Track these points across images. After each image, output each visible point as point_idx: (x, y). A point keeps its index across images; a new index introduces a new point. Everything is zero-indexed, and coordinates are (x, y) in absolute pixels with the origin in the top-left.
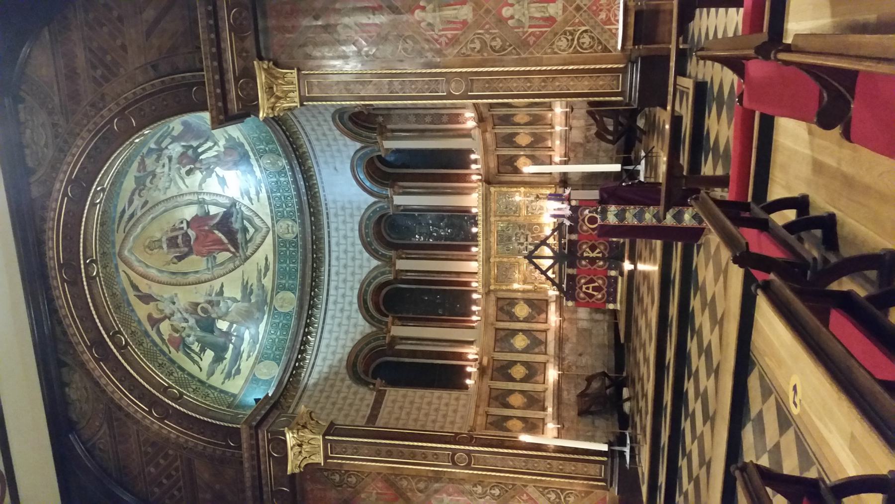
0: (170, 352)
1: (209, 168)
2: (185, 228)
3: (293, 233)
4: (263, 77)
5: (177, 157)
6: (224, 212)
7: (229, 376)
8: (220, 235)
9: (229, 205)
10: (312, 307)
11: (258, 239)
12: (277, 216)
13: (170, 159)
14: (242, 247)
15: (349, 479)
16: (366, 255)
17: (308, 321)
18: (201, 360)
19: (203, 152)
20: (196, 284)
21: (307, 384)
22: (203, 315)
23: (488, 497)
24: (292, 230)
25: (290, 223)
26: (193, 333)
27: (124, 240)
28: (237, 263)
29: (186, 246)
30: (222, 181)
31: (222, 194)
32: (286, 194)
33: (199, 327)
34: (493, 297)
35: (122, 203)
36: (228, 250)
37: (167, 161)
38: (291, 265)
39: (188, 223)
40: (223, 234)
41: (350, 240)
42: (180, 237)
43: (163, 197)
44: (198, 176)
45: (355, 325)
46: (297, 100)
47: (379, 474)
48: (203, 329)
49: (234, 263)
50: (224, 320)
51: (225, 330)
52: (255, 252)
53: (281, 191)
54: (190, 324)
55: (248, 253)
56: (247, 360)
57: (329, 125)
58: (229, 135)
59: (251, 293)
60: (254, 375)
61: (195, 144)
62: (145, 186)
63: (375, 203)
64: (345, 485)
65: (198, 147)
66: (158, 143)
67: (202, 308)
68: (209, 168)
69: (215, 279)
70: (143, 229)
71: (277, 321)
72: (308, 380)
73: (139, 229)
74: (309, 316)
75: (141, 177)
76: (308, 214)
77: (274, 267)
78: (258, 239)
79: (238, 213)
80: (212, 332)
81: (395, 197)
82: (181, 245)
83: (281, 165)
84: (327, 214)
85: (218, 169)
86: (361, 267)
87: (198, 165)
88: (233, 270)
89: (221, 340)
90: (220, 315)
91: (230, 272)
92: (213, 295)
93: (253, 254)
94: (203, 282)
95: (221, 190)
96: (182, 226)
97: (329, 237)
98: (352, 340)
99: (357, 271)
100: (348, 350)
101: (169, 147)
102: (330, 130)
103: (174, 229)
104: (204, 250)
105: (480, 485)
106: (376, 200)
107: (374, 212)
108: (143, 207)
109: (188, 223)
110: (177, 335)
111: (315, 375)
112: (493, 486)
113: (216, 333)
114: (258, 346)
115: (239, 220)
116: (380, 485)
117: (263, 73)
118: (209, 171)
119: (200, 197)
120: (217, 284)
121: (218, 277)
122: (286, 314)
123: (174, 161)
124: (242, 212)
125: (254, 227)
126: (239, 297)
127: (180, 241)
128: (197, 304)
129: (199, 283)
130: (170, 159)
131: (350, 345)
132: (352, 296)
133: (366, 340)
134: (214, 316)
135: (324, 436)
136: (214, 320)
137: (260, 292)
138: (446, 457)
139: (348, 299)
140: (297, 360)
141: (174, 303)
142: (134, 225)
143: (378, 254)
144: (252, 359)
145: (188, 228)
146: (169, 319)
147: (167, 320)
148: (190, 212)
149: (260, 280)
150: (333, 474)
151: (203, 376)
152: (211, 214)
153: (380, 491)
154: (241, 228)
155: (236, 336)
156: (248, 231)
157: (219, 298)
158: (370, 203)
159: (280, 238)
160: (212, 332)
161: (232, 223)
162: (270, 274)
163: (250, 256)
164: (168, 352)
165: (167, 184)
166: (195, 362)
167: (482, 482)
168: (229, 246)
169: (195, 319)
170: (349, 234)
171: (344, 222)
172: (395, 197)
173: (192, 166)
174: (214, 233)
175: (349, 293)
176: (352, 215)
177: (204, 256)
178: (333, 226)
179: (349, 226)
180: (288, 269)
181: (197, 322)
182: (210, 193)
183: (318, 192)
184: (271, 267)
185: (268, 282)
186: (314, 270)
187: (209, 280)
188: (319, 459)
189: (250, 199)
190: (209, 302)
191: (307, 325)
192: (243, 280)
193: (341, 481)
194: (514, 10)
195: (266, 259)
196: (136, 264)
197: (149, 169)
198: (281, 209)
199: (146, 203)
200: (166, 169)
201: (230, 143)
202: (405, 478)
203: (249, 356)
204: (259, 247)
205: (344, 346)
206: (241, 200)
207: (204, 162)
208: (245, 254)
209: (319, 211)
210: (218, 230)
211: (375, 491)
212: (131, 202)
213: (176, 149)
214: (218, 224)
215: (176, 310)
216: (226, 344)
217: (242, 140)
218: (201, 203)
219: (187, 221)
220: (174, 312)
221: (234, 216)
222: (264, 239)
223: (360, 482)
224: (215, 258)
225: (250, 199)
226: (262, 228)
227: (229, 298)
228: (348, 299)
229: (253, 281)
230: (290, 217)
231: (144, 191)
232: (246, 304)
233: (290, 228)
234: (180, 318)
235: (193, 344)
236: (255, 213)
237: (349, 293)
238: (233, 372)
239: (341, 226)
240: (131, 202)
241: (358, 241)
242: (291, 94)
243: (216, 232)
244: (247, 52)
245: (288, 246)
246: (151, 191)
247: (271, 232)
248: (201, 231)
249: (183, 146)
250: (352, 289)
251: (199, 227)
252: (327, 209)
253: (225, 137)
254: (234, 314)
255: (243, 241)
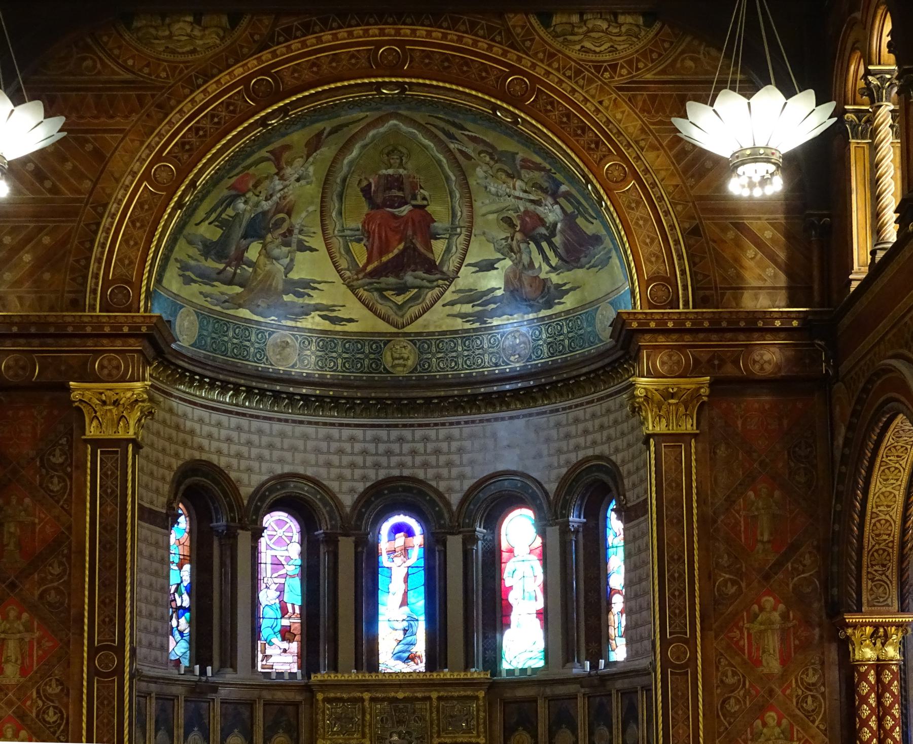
0: (230, 178)
1: (512, 250)
2: (414, 202)
3: (393, 366)
4: (688, 386)
5: (537, 212)
6: (435, 262)
7: (184, 267)
8: (396, 251)
9: (445, 269)
10: (277, 396)
11: (382, 308)
12: (421, 341)
13: (537, 203)
14: (371, 284)
15: (56, 480)
16: (361, 487)
17: (257, 391)
18: (210, 223)
19: (541, 250)
20: (322, 212)
21: (171, 395)
22: (273, 221)
23: (40, 703)
24: (399, 365)
25: (410, 363)
26: (249, 208)
27: (415, 121)
28: (348, 274)
29: (384, 199)
30: (488, 266)
31: (465, 263)
32: (460, 361)
33: (257, 215)
34: (299, 698)
35: (474, 130)
36: (369, 261)
37: (532, 197)
38: (340, 361)
39: (423, 207)
40: (397, 256)
41: (383, 460)
42: (400, 194)
43: (472, 182)
44: (501, 234)
45: (249, 470)
46: (658, 430)
47: (69, 528)
48: (253, 222)
49: (348, 269)
50: (260, 253)
51: (246, 254)
52: (363, 303)
53: (466, 353)
54: (264, 203)
55: (361, 292)
56: (201, 293)
57: (586, 448)
58: (567, 292)
59: (300, 295)
60: (182, 307)
61: (557, 240)
62: (496, 162)
63: (448, 504)
64: (44, 471)
65: (551, 245)
66: (567, 196)
67: (283, 220)
68: (512, 250)
69: (325, 240)
70: (426, 147)
71: (253, 338)
72: (176, 397)
73: (427, 142)
74: (262, 393)
75: (514, 160)
76: (429, 394)
77: (337, 333)
78: (382, 308)
79: (430, 281)
80: (245, 237)
81: (459, 539)
82: (387, 194)
83: (512, 358)
84: (428, 425)
85: (508, 263)
86: (340, 478)
87: (518, 236)
88: (336, 267)
89: (232, 251)
90: (269, 246)
91: (334, 263)
92: (301, 237)
93: (360, 299)
94: (322, 221)
95: (473, 262)
96: (419, 197)
97: (388, 426)
98: (229, 466)
99: (334, 472)
100: (214, 459)
101: (556, 207)
102: (577, 448)
103: (414, 186)
104: (374, 227)
105: (62, 690)
106: (454, 508)
107: (433, 503)
108: (461, 151)
109: (423, 207)
110: (250, 185)
111: (182, 408)
112: (61, 712)
113: (244, 242)
114: (218, 308)
115: (418, 282)
116: (49, 530)
117: (694, 386)
118: (506, 249)
119: (464, 230)
120: (317, 242)
121: (326, 245)
122: (261, 351)
123: (531, 207)
124: (432, 288)
125: (405, 303)
126: (294, 276)
127: (395, 193)
128: (289, 213)
129: (322, 216)
130: (537, 203)
131: (222, 462)
132: (293, 463)
133: (229, 487)
134: (269, 237)
135: (133, 441)
136: (261, 237)
137: (297, 310)
138: (107, 637)
139: (288, 456)
140: (203, 376)
141: (298, 180)
142: (436, 136)
143: (363, 506)
144: (201, 301)
145: (414, 206)
146: (277, 174)
147: (276, 171)
148: (437, 209)
149: (317, 308)
150: (63, 453)
151: (190, 229)
152: (433, 242)
153: (38, 528)
154: (405, 284)
155: (235, 273)
156: (398, 295)
157: (294, 246)
158: (447, 496)
159: (385, 344)
160: (245, 237)
161: (414, 271)
162: (326, 325)
163: (356, 295)
164: (231, 175)
165: (493, 190)
166: (208, 214)
167: (68, 695)
168: (376, 264)
169: (268, 211)
170: (394, 460)
171: (414, 453)
172: (459, 539)
173: (518, 229)
174: (400, 243)
175: (299, 457)
176: (425, 465)
177: (363, 226)
178: (407, 433)
179: (408, 460)
180: (334, 355)
181: (264, 213)
182: (468, 246)
183: (465, 414)
184: (338, 328)
185: (314, 321)
186: (335, 399)
187: (324, 231)
188: (92, 431)
189: (452, 303)
190: (290, 231)
191: (250, 391)
192: (319, 283)
193: (54, 467)
194: (773, 728)
195: (351, 320)
196: (371, 134)
197: (523, 172)
198: (434, 350)
199: (468, 157)
200: (518, 193)
201: (552, 289)
202: (64, 571)
203: (206, 295)
204: (371, 309)
205: (219, 452)
206: (452, 288)
207: (523, 246)
208: (362, 286)
209: (433, 411)
210: (405, 249)
211: (37, 521)
212: (474, 139)
213: (552, 213)
214: (415, 249)
215: (287, 183)
216: (226, 258)
217: (558, 309)
218: (452, 231)
219: (425, 206)
220: (285, 180)
221: (425, 275)
222: (383, 319)
223: (52, 497)
224: (359, 241)
225: (452, 303)
226: (402, 316)
227: (292, 260)
228: (288, 456)
229: (317, 298)
230: (420, 362)
231: (488, 158)
232: (280, 287)
233: (401, 362)
234: (274, 189)
235: (234, 209)
236: (428, 309)
237: (299, 457)
238: (188, 273)
239: (406, 447)
240: (474, 139)
241: (382, 474)
242: (664, 421)
243: (401, 247)
244: (720, 366)
245: (372, 356)
246: (485, 168)
247: (395, 330)
248: (406, 223)
249: (555, 225)
250: (305, 463)
251: (413, 220)
252: (436, 425)
253: (565, 284)
254: (268, 267)
255: (383, 286)
